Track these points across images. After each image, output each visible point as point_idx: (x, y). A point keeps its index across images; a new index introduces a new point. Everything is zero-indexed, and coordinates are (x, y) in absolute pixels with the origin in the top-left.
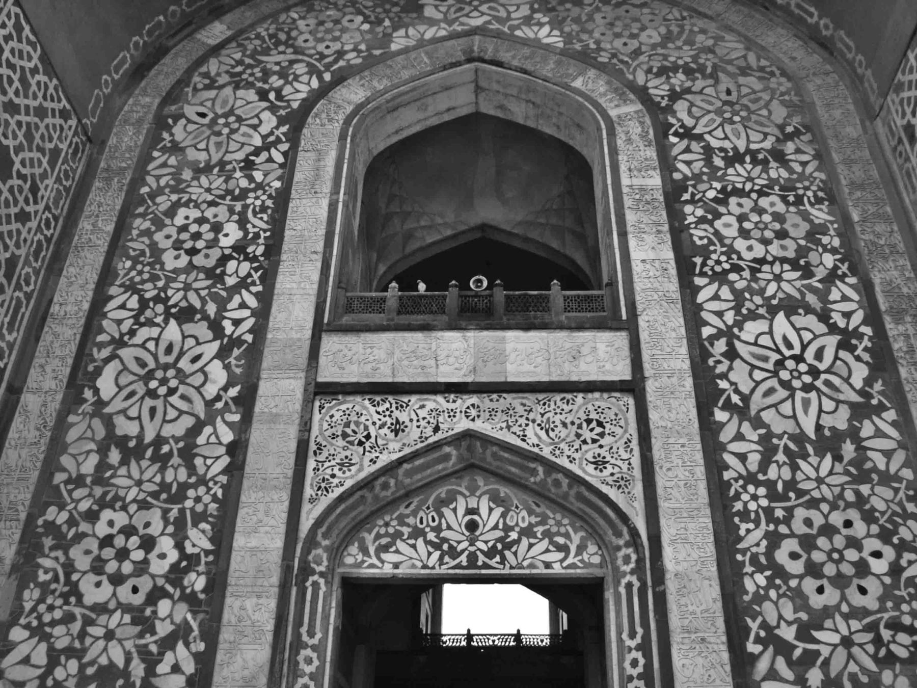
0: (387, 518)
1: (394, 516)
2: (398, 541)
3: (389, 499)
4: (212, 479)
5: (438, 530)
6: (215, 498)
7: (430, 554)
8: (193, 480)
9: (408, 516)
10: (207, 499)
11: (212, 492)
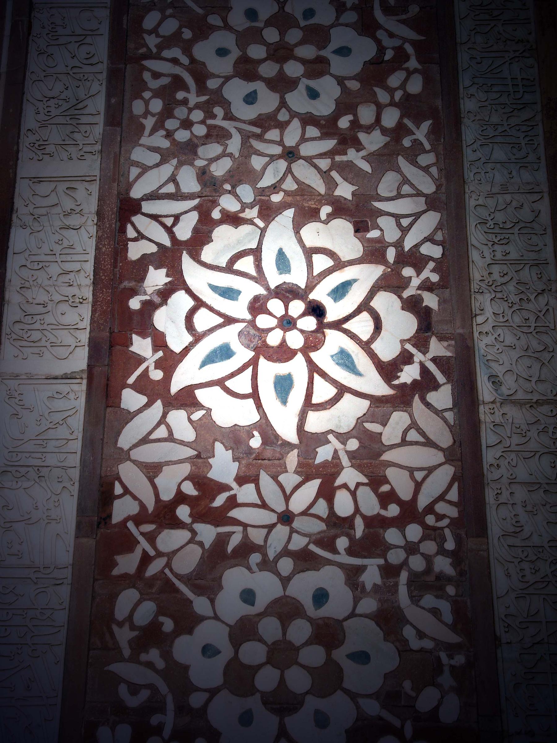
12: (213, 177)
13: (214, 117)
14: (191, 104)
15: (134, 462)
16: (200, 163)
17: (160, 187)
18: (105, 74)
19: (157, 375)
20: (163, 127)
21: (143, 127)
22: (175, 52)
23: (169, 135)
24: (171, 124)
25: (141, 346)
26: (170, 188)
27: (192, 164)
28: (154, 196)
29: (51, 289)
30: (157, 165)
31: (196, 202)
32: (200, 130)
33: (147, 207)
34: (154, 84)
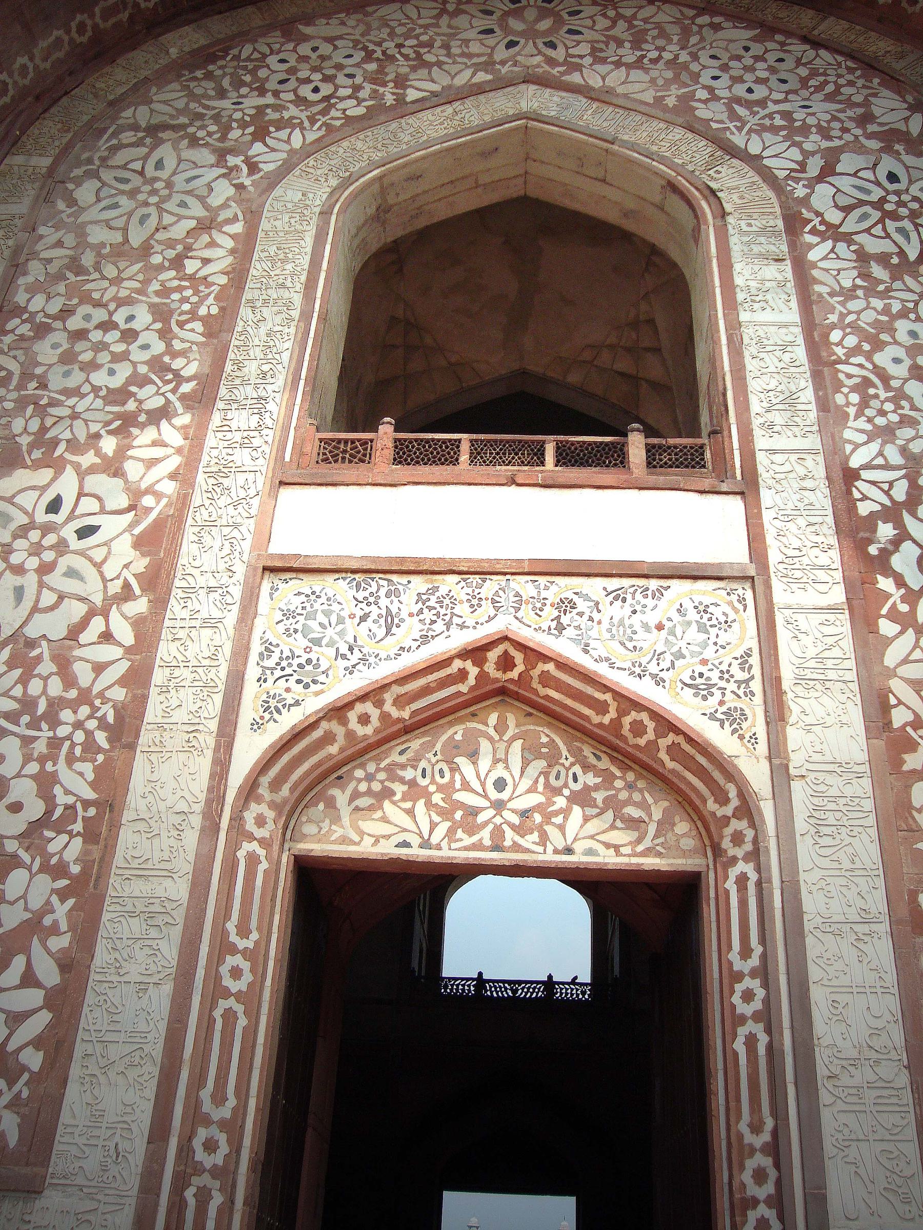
0: (371, 767)
1: (382, 766)
2: (387, 804)
3: (370, 741)
4: (101, 694)
5: (447, 790)
6: (103, 724)
7: (433, 826)
8: (73, 694)
9: (403, 767)
10: (92, 724)
11: (99, 714)
12: (913, 453)
13: (903, 408)
14: (882, 397)
15: (901, 678)
16: (901, 442)
17: (873, 459)
18: (808, 374)
19: (904, 608)
20: (863, 414)
21: (848, 415)
22: (860, 360)
23: (870, 420)
24: (869, 412)
25: (885, 584)
26: (880, 461)
27: (894, 443)
28: (868, 466)
29: (802, 537)
30: (866, 443)
31: (904, 471)
32: (894, 418)
33: (864, 474)
34: (850, 382)
